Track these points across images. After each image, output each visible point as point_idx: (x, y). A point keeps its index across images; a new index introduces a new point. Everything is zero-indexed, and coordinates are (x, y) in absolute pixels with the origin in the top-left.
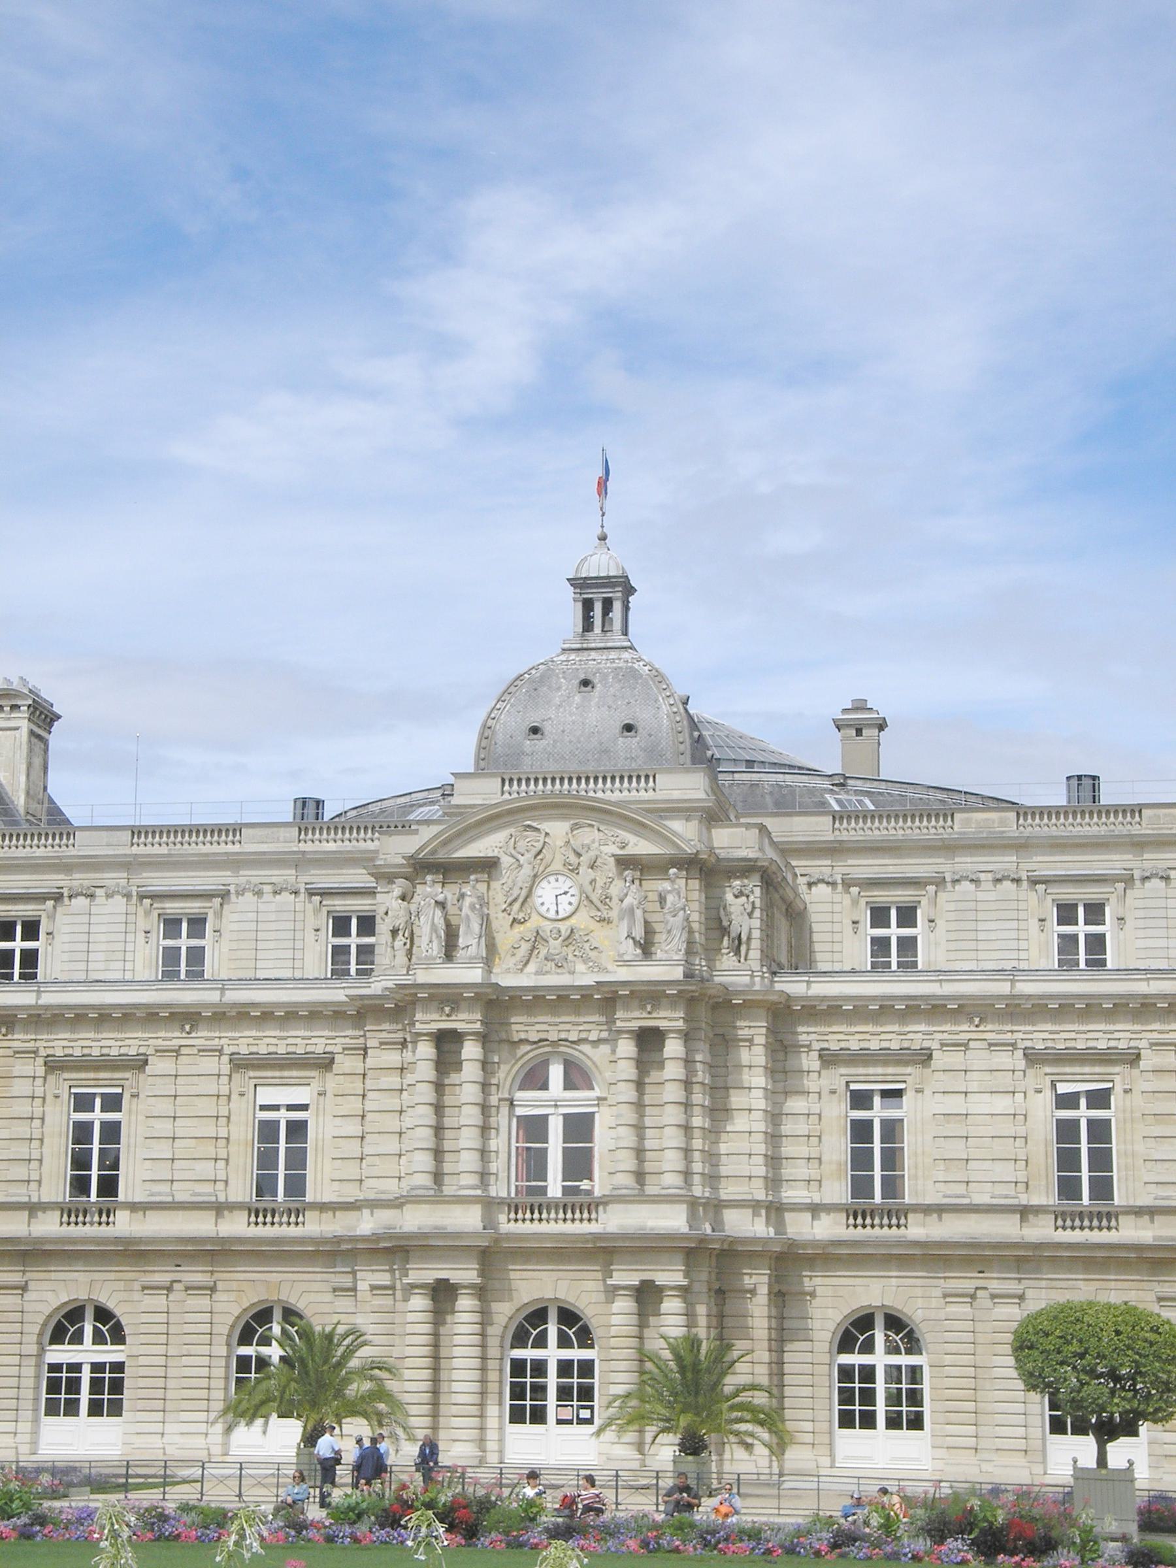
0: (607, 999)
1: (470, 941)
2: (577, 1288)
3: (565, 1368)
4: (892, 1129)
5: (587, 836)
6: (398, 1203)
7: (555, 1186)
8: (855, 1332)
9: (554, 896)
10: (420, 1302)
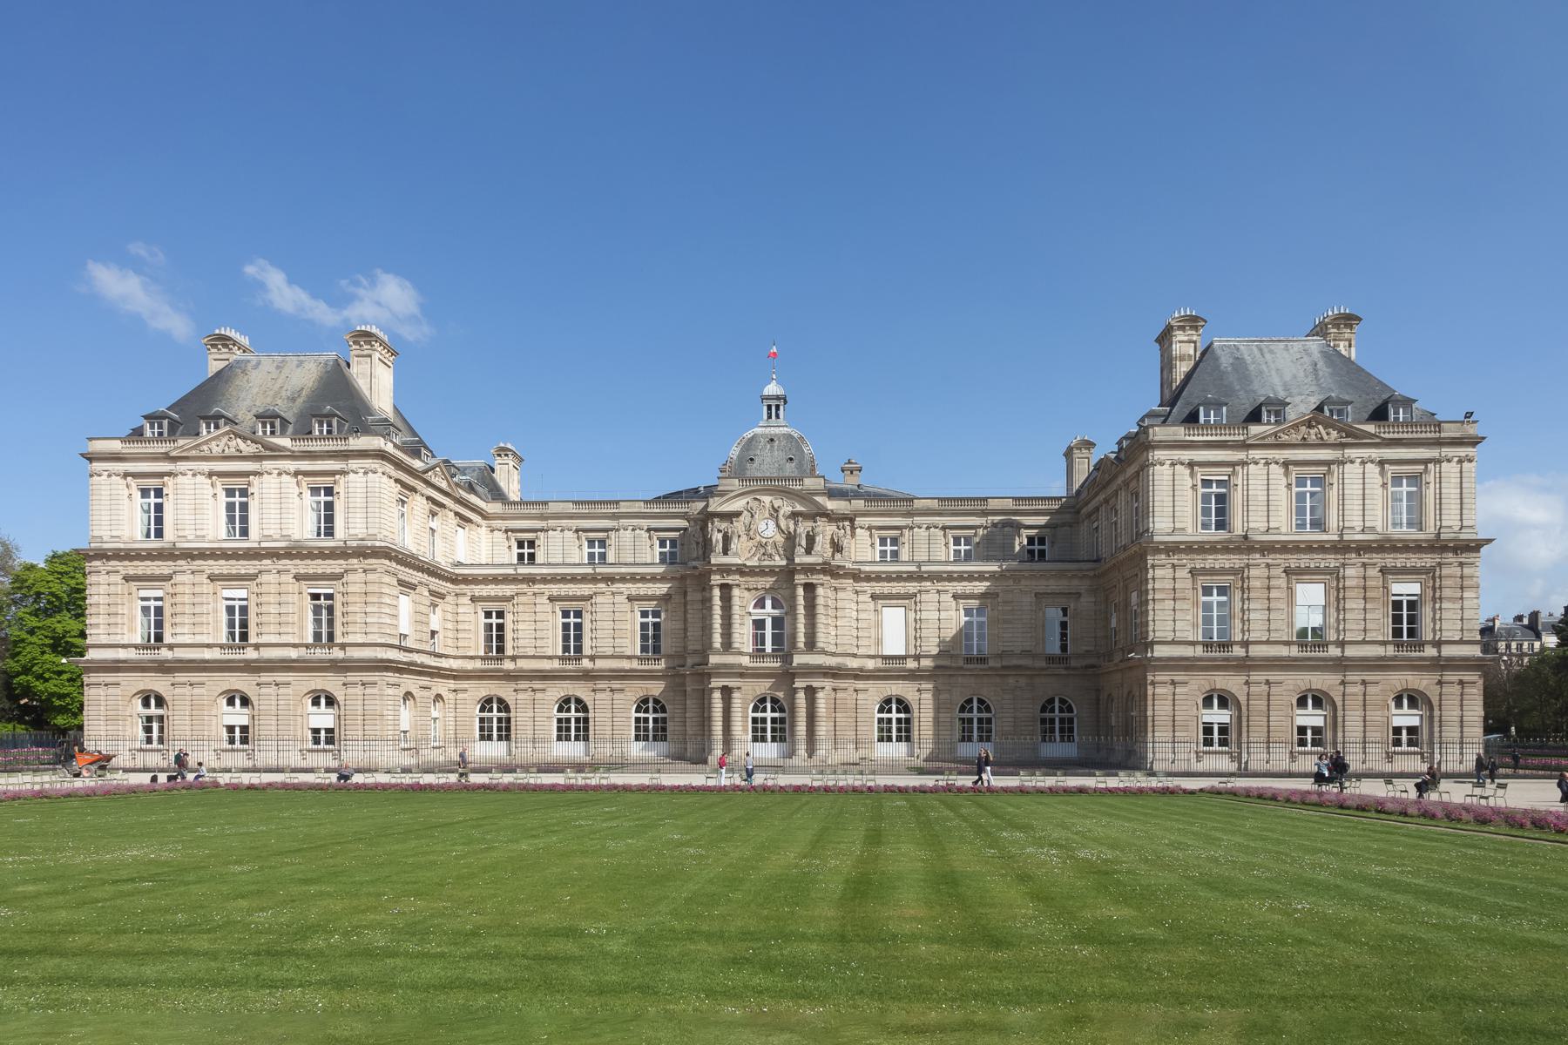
3: (774, 720)
7: (769, 648)
9: (768, 530)
10: (717, 695)
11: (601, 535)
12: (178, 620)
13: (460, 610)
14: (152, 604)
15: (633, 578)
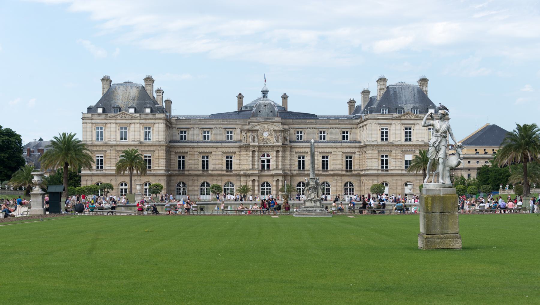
0: (273, 147)
1: (256, 140)
2: (270, 180)
3: (267, 189)
4: (303, 161)
5: (269, 127)
6: (247, 170)
7: (266, 168)
8: (299, 185)
9: (265, 134)
10: (251, 182)
11: (208, 130)
12: (109, 163)
13: (172, 156)
14: (100, 158)
15: (225, 147)
